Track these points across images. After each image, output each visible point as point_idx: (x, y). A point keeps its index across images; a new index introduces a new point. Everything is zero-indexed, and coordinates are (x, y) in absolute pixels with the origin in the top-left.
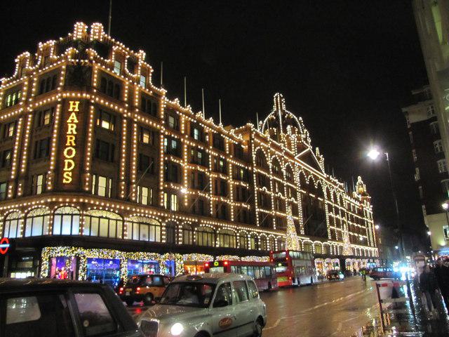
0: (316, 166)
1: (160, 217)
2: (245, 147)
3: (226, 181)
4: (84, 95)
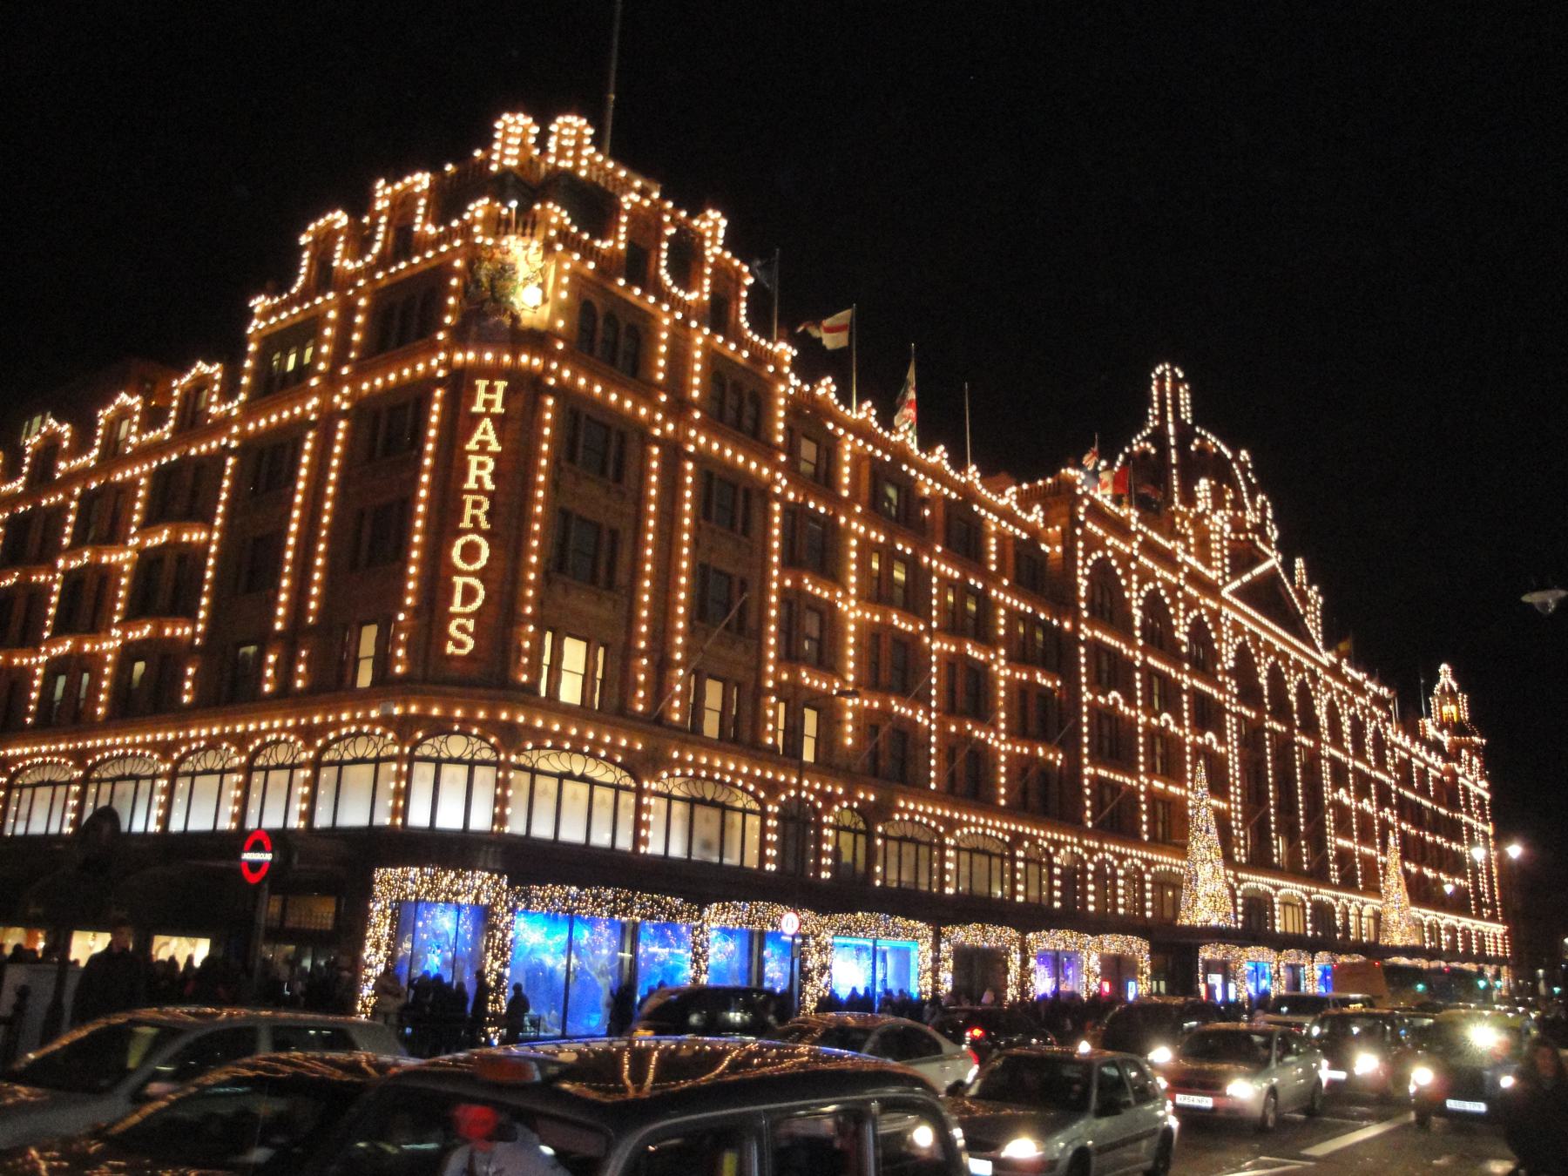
0: (1294, 624)
1: (762, 783)
3: (986, 665)
4: (524, 359)
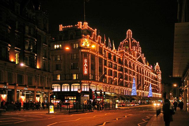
0: (142, 62)
2: (121, 59)
4: (88, 51)
